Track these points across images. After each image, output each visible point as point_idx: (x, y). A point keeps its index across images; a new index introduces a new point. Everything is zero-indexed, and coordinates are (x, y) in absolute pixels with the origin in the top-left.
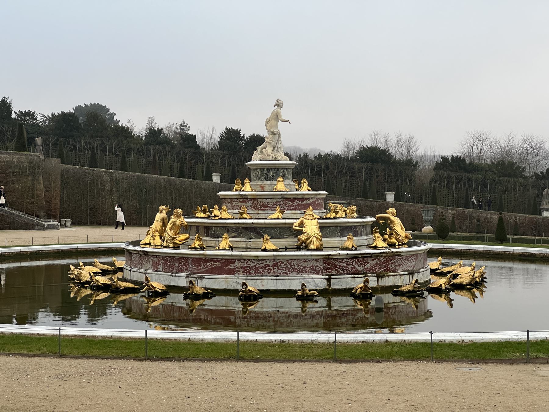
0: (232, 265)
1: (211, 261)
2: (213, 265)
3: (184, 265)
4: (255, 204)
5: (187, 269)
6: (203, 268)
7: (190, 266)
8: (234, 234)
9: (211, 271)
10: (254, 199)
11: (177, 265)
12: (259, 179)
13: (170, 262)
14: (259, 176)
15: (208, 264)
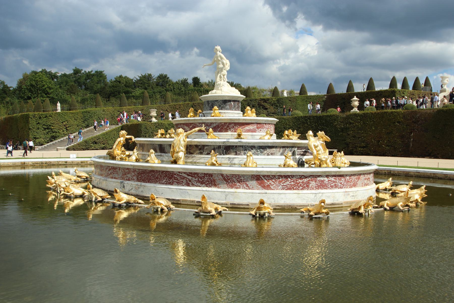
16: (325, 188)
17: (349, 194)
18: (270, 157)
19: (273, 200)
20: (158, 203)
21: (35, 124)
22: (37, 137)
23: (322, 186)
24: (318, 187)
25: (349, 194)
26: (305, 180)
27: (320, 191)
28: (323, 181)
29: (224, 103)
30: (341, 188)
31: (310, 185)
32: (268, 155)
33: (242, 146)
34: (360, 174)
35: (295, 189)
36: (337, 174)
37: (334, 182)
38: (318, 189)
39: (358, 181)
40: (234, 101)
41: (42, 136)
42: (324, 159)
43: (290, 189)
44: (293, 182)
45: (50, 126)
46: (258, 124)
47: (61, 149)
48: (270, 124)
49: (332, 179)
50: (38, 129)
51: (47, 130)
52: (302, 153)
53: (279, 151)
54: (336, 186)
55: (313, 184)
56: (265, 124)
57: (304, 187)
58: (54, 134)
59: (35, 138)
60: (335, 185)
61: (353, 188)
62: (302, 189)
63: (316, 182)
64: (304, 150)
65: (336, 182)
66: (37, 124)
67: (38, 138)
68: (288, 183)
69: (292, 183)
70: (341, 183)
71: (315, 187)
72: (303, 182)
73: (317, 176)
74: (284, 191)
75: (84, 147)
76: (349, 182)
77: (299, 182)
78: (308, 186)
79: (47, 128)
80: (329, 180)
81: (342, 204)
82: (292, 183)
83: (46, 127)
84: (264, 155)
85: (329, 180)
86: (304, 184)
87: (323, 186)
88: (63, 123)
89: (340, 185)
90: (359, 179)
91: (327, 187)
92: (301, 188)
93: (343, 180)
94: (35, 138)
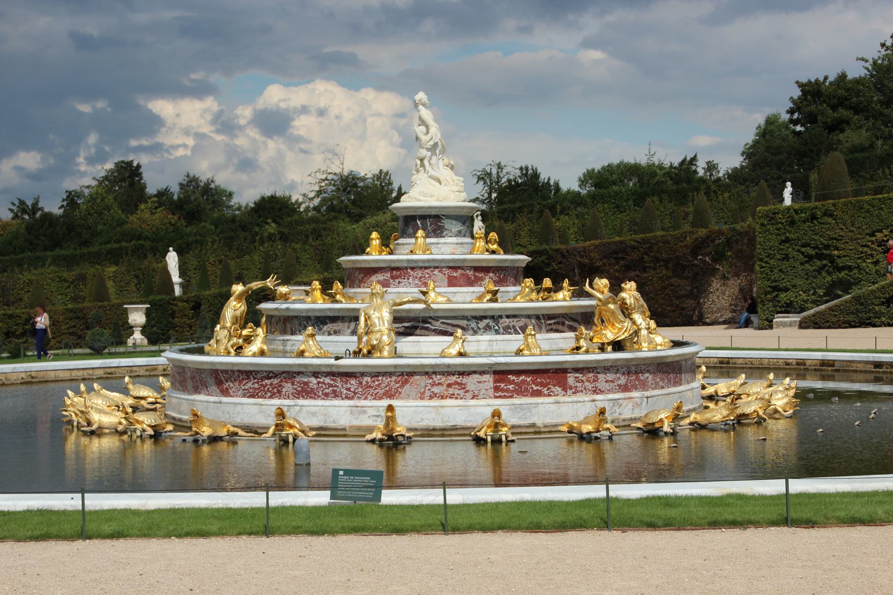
16: (311, 398)
17: (365, 412)
18: (333, 338)
19: (228, 416)
20: (138, 422)
21: (774, 241)
22: (782, 285)
23: (306, 392)
24: (298, 395)
25: (365, 412)
26: (275, 381)
27: (301, 402)
28: (306, 384)
29: (433, 221)
30: (348, 398)
31: (284, 390)
32: (330, 334)
33: (296, 317)
34: (411, 374)
35: (261, 397)
36: (334, 370)
37: (331, 386)
38: (298, 398)
39: (402, 386)
40: (423, 218)
41: (799, 282)
42: (375, 342)
43: (252, 396)
44: (258, 383)
45: (827, 247)
46: (393, 269)
47: (784, 325)
48: (426, 268)
49: (327, 380)
50: (786, 258)
51: (819, 263)
52: (401, 330)
53: (349, 327)
54: (336, 395)
55: (288, 387)
56: (413, 268)
57: (274, 394)
58: (843, 273)
59: (776, 289)
60: (334, 392)
61: (382, 401)
62: (271, 397)
63: (293, 384)
64: (406, 325)
65: (336, 386)
66: (783, 242)
67: (786, 290)
68: (250, 384)
69: (256, 386)
70: (349, 389)
71: (292, 394)
72: (271, 384)
73: (295, 373)
74: (246, 400)
75: (851, 318)
76: (371, 387)
77: (266, 385)
78: (279, 392)
79: (820, 257)
80: (319, 383)
81: (344, 429)
82: (256, 386)
83: (813, 253)
84: (323, 334)
85: (319, 383)
86: (273, 389)
87: (307, 393)
88: (873, 235)
89: (345, 392)
90: (406, 382)
91: (315, 394)
92: (269, 394)
93: (353, 382)
94: (776, 289)
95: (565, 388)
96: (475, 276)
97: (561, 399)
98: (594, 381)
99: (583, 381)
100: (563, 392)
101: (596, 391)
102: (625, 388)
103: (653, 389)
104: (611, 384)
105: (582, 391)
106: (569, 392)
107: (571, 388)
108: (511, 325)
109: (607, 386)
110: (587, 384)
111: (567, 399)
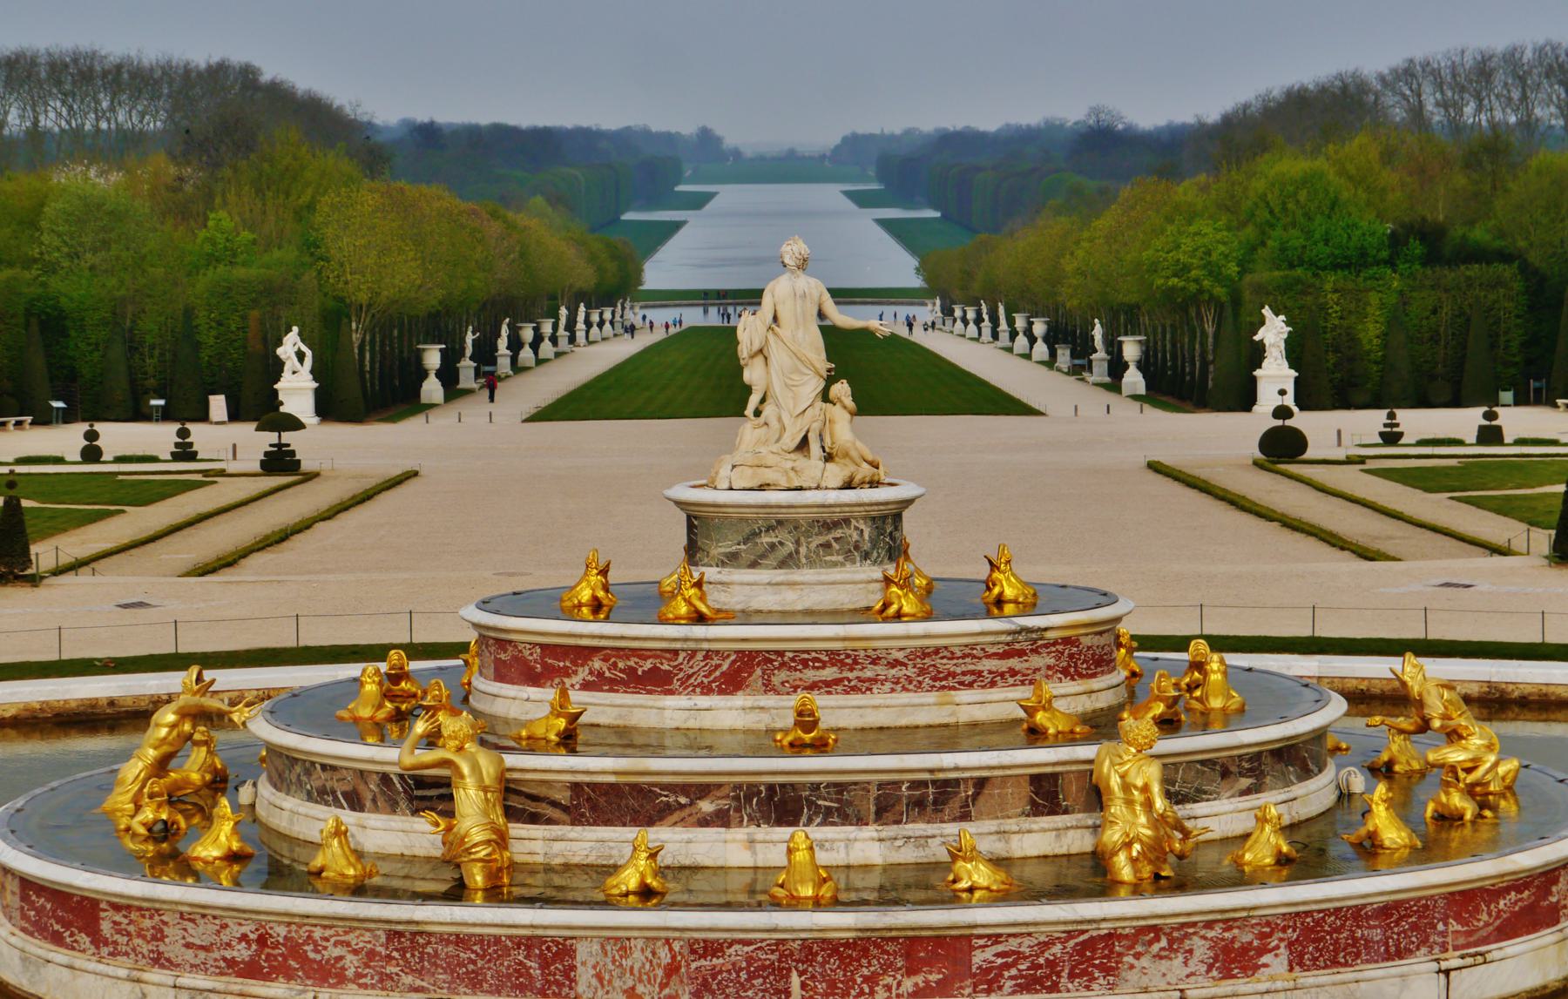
0: (1554, 889)
1: (1507, 890)
2: (1516, 903)
3: (1414, 927)
4: (1071, 656)
5: (1424, 941)
6: (1487, 924)
7: (1440, 927)
8: (1245, 782)
9: (1509, 929)
10: (1067, 641)
11: (1377, 935)
12: (866, 556)
13: (1338, 930)
14: (867, 546)
15: (1502, 903)
95: (98, 940)
96: (544, 665)
97: (80, 961)
98: (154, 938)
99: (129, 934)
100: (93, 949)
101: (159, 960)
102: (251, 970)
103: (365, 986)
104: (202, 955)
105: (127, 954)
106: (105, 951)
107: (106, 944)
108: (328, 785)
109: (189, 955)
110: (138, 941)
111: (93, 966)
